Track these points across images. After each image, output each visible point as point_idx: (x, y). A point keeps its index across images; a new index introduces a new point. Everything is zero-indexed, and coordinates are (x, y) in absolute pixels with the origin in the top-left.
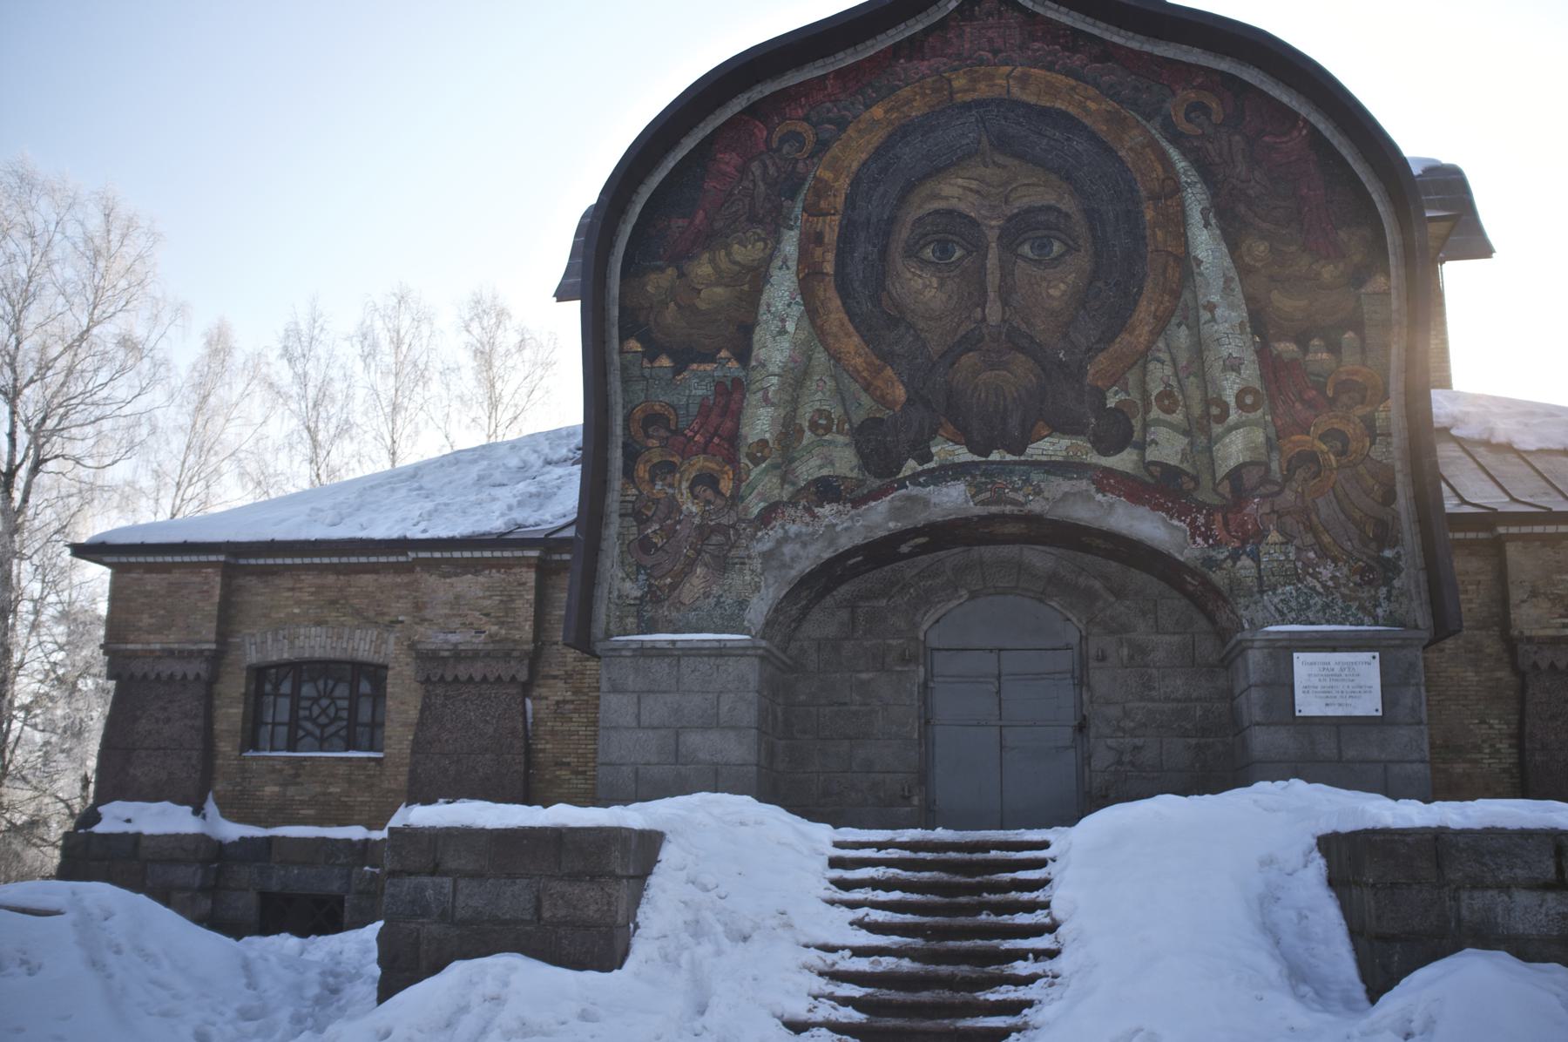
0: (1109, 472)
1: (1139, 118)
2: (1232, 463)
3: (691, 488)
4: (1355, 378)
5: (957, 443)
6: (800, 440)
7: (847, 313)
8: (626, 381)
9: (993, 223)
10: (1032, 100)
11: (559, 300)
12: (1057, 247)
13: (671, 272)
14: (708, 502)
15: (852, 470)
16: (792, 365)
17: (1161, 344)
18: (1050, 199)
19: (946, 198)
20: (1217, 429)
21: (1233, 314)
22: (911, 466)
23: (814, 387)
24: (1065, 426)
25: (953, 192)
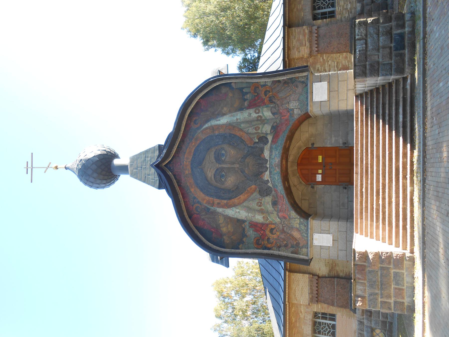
0: (272, 141)
1: (196, 134)
2: (271, 115)
3: (273, 234)
4: (253, 89)
5: (265, 174)
6: (263, 209)
7: (235, 198)
8: (249, 248)
9: (217, 166)
10: (192, 157)
11: (229, 267)
12: (223, 152)
13: (224, 237)
14: (277, 231)
15: (270, 198)
16: (246, 211)
17: (245, 130)
18: (213, 153)
19: (211, 175)
20: (263, 118)
21: (239, 114)
22: (270, 185)
23: (251, 206)
24: (262, 150)
25: (210, 174)
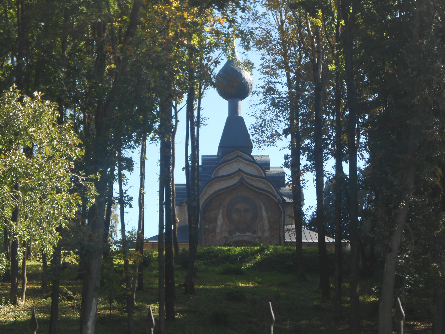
22: (234, 235)
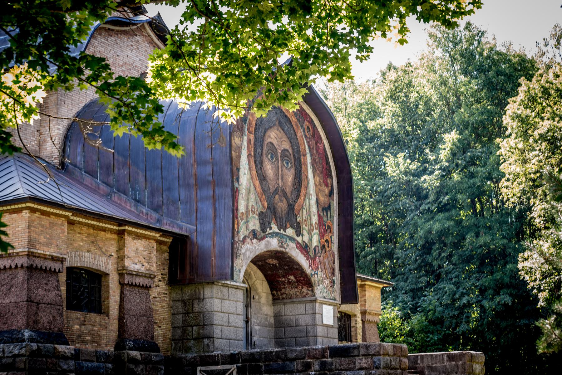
22: (268, 231)
